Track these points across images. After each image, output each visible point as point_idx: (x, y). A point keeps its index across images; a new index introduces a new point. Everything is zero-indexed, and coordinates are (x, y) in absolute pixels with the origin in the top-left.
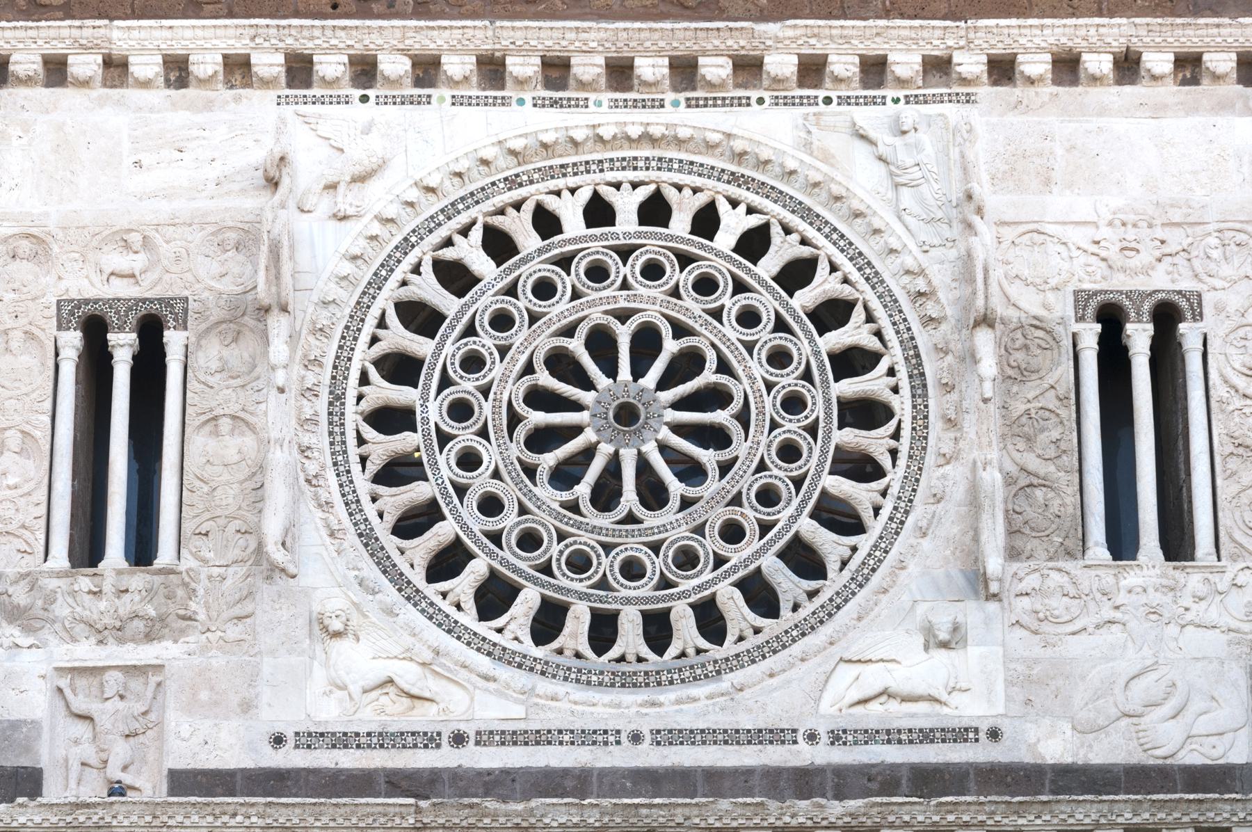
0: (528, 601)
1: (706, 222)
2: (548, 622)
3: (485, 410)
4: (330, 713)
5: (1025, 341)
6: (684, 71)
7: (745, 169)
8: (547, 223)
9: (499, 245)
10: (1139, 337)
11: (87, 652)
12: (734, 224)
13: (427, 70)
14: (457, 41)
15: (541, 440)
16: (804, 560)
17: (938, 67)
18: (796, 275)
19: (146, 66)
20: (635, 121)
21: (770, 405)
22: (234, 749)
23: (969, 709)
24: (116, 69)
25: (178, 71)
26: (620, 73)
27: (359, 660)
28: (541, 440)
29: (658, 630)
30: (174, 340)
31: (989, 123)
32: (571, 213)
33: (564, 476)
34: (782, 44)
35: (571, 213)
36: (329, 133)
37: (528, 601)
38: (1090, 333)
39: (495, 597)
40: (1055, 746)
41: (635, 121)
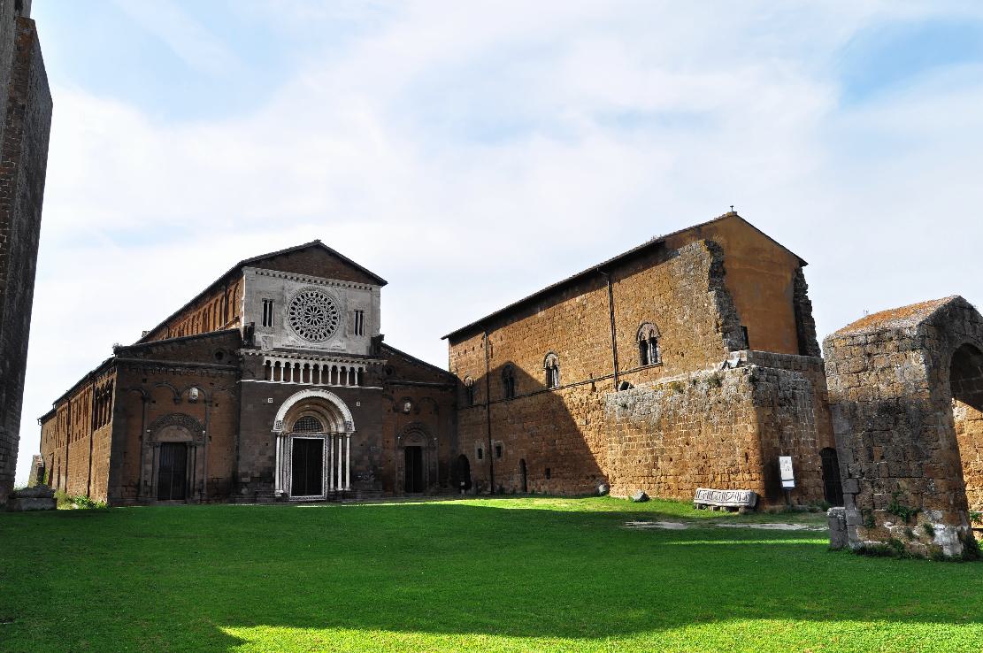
0: (304, 333)
1: (322, 297)
2: (306, 335)
5: (350, 313)
6: (321, 282)
15: (306, 317)
16: (329, 332)
17: (344, 285)
18: (329, 303)
19: (271, 275)
20: (316, 286)
22: (278, 345)
24: (268, 274)
26: (315, 282)
27: (291, 338)
32: (309, 295)
35: (309, 295)
37: (304, 333)
39: (302, 332)
40: (350, 352)
41: (316, 286)
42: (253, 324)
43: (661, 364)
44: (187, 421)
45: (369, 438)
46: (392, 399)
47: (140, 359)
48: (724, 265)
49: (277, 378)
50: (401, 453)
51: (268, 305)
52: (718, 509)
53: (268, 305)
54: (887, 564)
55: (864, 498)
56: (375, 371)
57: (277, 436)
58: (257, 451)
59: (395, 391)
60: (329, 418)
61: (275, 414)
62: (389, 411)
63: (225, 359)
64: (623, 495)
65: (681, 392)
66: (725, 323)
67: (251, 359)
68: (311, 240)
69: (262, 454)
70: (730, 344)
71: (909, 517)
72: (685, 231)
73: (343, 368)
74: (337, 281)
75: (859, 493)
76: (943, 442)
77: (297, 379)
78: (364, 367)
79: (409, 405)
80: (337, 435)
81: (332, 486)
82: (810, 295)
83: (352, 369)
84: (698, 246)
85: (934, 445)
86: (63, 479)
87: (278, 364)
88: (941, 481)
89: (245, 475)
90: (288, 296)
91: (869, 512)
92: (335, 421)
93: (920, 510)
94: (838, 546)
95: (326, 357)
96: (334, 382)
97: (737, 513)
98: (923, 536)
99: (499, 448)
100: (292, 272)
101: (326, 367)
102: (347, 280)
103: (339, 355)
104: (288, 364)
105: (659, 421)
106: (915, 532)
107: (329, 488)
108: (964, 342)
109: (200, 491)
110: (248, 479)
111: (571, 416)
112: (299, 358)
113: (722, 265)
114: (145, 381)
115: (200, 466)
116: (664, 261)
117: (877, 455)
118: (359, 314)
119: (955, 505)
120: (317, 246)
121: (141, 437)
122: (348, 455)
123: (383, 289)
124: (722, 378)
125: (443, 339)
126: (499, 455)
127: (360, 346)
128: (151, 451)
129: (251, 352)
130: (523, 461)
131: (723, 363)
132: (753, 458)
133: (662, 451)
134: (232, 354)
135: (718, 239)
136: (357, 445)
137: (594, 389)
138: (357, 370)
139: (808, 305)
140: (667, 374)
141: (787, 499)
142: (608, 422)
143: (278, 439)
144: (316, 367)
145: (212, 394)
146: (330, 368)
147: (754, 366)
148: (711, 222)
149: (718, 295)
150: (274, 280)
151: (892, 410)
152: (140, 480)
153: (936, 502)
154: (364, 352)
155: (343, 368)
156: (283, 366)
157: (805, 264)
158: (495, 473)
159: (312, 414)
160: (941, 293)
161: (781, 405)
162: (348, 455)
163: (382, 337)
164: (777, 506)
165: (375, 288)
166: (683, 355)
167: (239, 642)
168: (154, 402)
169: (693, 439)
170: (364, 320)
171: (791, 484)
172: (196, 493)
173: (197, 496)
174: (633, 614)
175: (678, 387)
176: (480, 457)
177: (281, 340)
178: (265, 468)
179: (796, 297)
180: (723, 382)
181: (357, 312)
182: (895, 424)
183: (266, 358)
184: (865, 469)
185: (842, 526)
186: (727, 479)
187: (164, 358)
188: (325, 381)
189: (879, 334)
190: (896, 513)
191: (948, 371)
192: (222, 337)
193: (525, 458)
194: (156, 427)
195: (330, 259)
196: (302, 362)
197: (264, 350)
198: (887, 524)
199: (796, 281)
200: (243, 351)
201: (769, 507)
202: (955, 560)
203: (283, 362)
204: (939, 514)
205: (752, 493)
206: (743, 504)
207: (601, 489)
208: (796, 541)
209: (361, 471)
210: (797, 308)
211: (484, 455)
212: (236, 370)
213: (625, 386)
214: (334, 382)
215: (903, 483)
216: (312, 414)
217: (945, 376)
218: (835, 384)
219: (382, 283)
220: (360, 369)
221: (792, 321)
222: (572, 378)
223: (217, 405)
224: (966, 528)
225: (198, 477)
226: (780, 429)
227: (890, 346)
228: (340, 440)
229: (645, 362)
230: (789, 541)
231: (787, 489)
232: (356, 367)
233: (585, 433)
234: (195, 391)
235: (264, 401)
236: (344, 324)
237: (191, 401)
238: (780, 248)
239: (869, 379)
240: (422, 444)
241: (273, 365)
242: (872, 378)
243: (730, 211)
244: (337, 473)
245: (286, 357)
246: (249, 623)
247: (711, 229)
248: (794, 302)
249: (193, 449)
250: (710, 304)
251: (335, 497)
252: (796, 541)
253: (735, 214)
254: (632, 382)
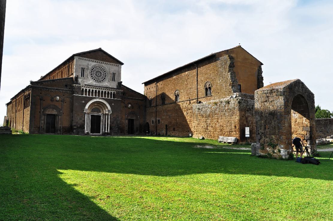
1: (101, 68)
2: (96, 81)
4: (89, 83)
5: (111, 74)
7: (103, 66)
8: (96, 67)
10: (114, 74)
11: (82, 80)
13: (93, 61)
14: (94, 60)
15: (96, 74)
23: (109, 85)
25: (85, 60)
26: (99, 62)
27: (91, 81)
28: (96, 74)
30: (85, 69)
31: (110, 66)
34: (105, 62)
36: (90, 63)
42: (78, 76)
43: (212, 96)
44: (55, 107)
45: (116, 116)
46: (124, 103)
47: (39, 86)
48: (234, 64)
49: (86, 94)
50: (127, 121)
51: (83, 70)
52: (225, 143)
53: (83, 70)
54: (265, 160)
55: (262, 140)
56: (119, 94)
57: (85, 114)
58: (79, 118)
59: (126, 100)
60: (103, 108)
61: (85, 106)
62: (123, 107)
63: (68, 87)
64: (197, 137)
65: (217, 105)
66: (233, 83)
67: (77, 88)
68: (97, 48)
69: (80, 119)
70: (234, 90)
71: (274, 147)
72: (223, 51)
73: (108, 92)
74: (106, 63)
75: (261, 139)
76: (286, 125)
77: (92, 95)
78: (115, 92)
79: (130, 105)
80: (106, 114)
81: (104, 131)
82: (263, 75)
83: (111, 93)
84: (226, 57)
85: (284, 125)
86: (14, 124)
87: (86, 90)
88: (284, 136)
89: (75, 126)
90: (90, 67)
91: (263, 145)
92: (105, 109)
93: (277, 145)
94: (253, 155)
95: (103, 88)
96: (105, 96)
97: (230, 144)
98: (277, 152)
99: (159, 121)
100: (91, 58)
101: (102, 92)
102: (111, 62)
103: (107, 88)
104: (89, 90)
105: (209, 114)
106: (275, 151)
107: (103, 131)
108: (299, 94)
109: (60, 131)
110: (76, 127)
111: (182, 111)
112: (93, 88)
113: (233, 64)
114: (41, 93)
115: (60, 122)
116: (215, 61)
117: (267, 128)
118: (114, 74)
119: (288, 143)
120: (100, 50)
121: (40, 112)
122: (109, 121)
123: (122, 66)
124: (230, 101)
125: (142, 84)
126: (159, 123)
127: (114, 85)
128: (43, 117)
129: (77, 85)
130: (166, 126)
131: (231, 96)
132: (238, 127)
133: (210, 124)
134: (71, 85)
135: (233, 55)
136: (112, 118)
137: (190, 103)
138: (113, 93)
139: (262, 78)
140: (214, 99)
141: (247, 140)
142: (193, 114)
143: (86, 114)
144: (99, 91)
145: (64, 99)
146: (104, 92)
147: (240, 98)
148: (232, 49)
149: (231, 74)
150: (84, 61)
151: (273, 114)
152: (40, 126)
153: (282, 143)
154: (115, 87)
155: (108, 92)
156: (88, 90)
157: (263, 64)
158: (157, 129)
159: (97, 107)
160: (293, 78)
161: (248, 111)
162: (109, 121)
163: (121, 82)
164: (243, 143)
165: (119, 65)
166: (219, 93)
167: (62, 173)
168: (44, 101)
169: (219, 121)
170: (116, 76)
171: (249, 136)
172: (59, 131)
173: (59, 132)
174: (180, 171)
175: (216, 104)
176: (153, 123)
177: (87, 82)
178: (81, 124)
179: (258, 75)
180: (230, 103)
181: (113, 73)
182: (273, 118)
183: (82, 88)
184: (263, 132)
185: (255, 149)
186: (229, 134)
187: (48, 86)
188: (102, 96)
189: (271, 90)
190: (270, 146)
191: (291, 103)
192: (67, 80)
193: (167, 124)
194: (45, 109)
195: (105, 55)
196: (94, 90)
197: (81, 85)
198: (268, 149)
199: (259, 70)
200: (74, 85)
201: (241, 143)
202: (286, 159)
203: (88, 89)
204: (282, 146)
205: (236, 138)
206: (233, 142)
207: (190, 135)
208: (243, 153)
209: (114, 126)
210: (258, 79)
211: (154, 123)
212: (71, 91)
213: (200, 102)
214: (105, 96)
215: (274, 137)
216: (97, 107)
217: (290, 105)
218: (257, 105)
219: (122, 64)
220: (114, 93)
221: (256, 83)
222: (183, 99)
223: (65, 103)
224: (290, 151)
225: (59, 126)
226: (247, 119)
227: (274, 94)
228: (107, 116)
229: (207, 95)
230: (241, 153)
231: (247, 137)
232: (113, 92)
233: (186, 117)
234: (58, 98)
235: (81, 102)
236: (109, 77)
237: (57, 101)
238: (255, 59)
239: (267, 104)
240: (134, 118)
241: (84, 90)
242: (268, 104)
243: (239, 45)
244: (105, 126)
245: (89, 87)
246: (66, 169)
247: (231, 51)
248: (258, 77)
249: (58, 117)
250: (228, 77)
251: (104, 134)
252: (243, 153)
253: (240, 47)
254: (202, 101)
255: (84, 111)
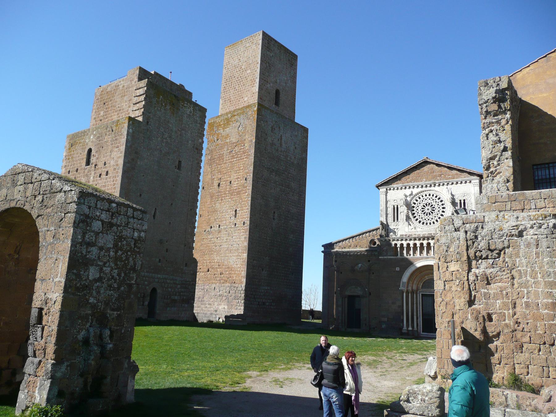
1: (433, 195)
3: (419, 210)
8: (423, 196)
9: (420, 198)
10: (462, 202)
12: (435, 195)
15: (423, 211)
21: (437, 208)
29: (430, 224)
32: (424, 195)
33: (424, 214)
35: (424, 195)
36: (408, 192)
38: (459, 202)
39: (420, 222)
53: (396, 209)
110: (386, 319)
143: (405, 294)
183: (393, 243)
255: (399, 286)
